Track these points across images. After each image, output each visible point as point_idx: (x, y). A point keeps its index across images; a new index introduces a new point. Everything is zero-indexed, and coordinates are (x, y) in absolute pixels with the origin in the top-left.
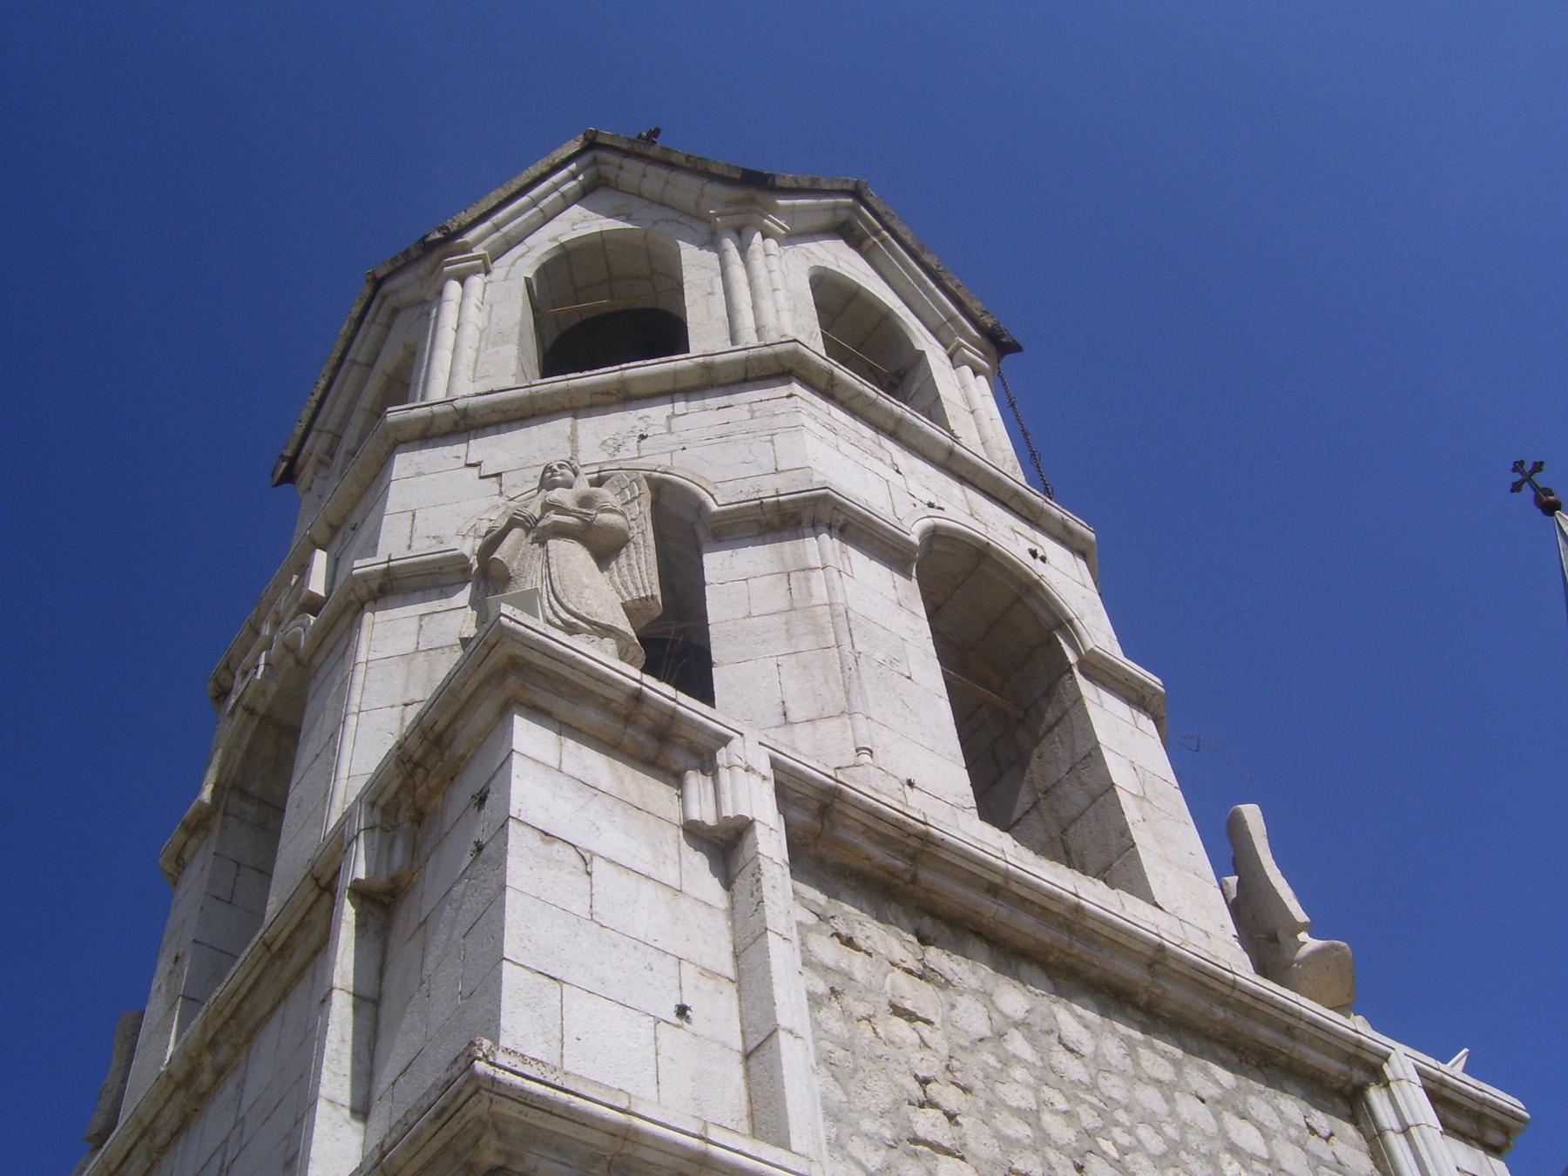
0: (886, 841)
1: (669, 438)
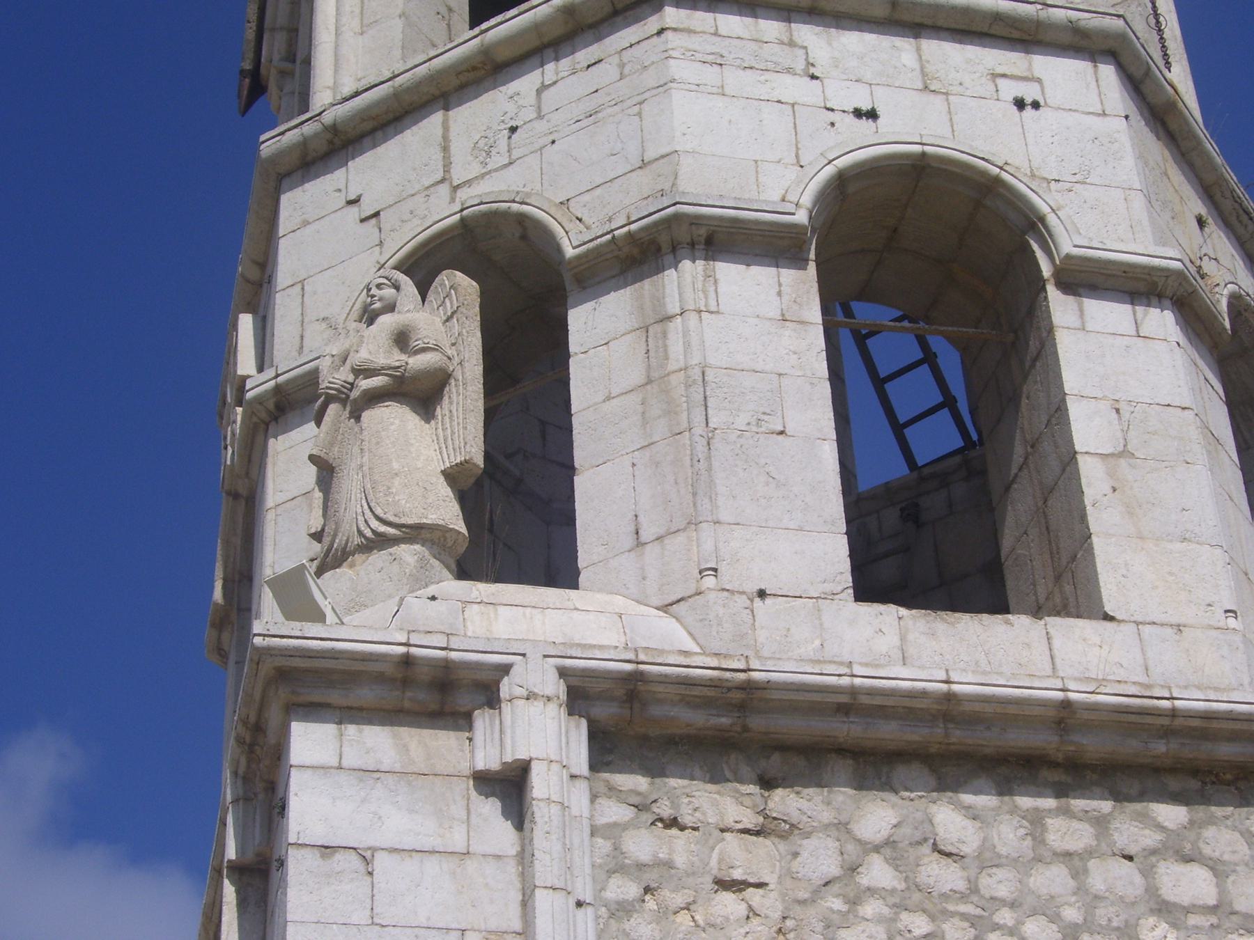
0: (706, 704)
1: (541, 126)
